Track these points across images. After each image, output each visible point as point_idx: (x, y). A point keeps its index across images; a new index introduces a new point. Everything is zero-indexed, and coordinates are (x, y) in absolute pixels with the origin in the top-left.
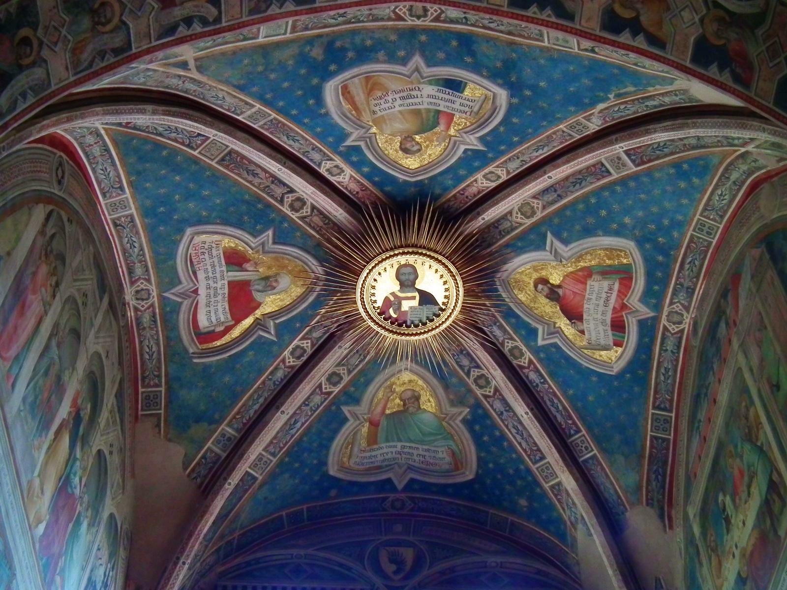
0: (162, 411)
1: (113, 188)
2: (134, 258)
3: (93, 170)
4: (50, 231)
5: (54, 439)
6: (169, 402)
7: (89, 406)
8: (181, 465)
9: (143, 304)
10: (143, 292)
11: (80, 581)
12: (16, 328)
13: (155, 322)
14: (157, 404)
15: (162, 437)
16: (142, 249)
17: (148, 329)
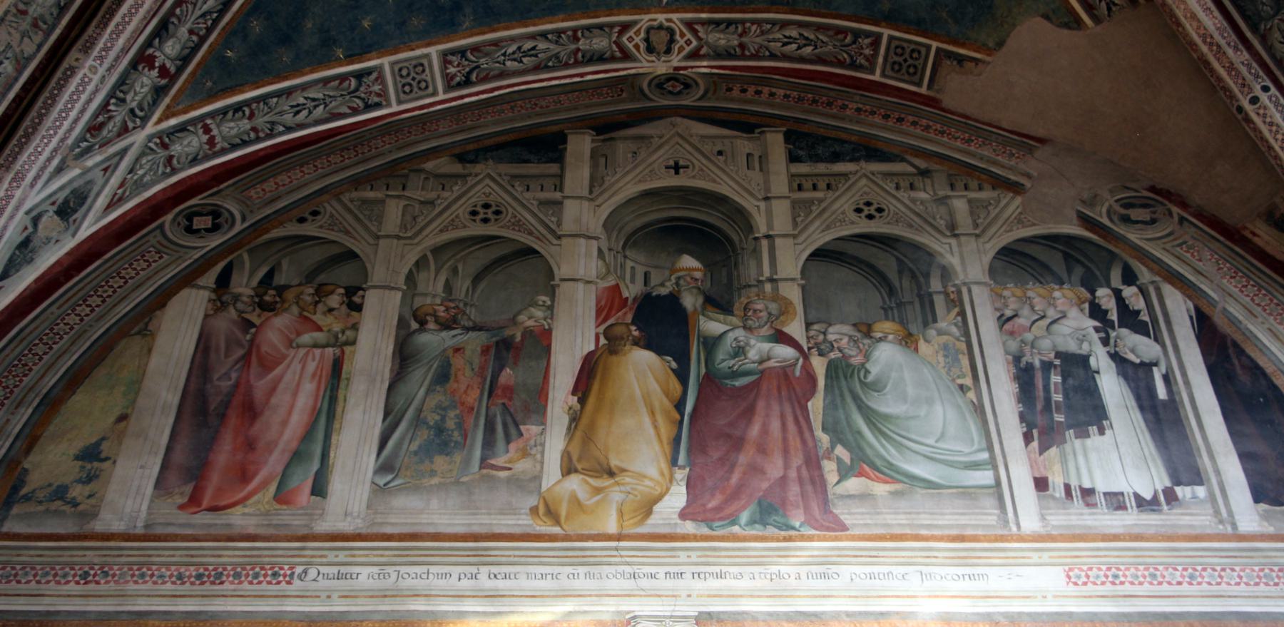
0: (935, 45)
1: (357, 90)
2: (564, 52)
3: (289, 129)
4: (243, 285)
5: (582, 401)
6: (920, 26)
7: (688, 262)
8: (1066, 32)
9: (682, 42)
10: (653, 38)
11: (979, 409)
12: (250, 445)
13: (730, 23)
14: (917, 50)
15: (988, 59)
16: (544, 35)
17: (744, 40)
